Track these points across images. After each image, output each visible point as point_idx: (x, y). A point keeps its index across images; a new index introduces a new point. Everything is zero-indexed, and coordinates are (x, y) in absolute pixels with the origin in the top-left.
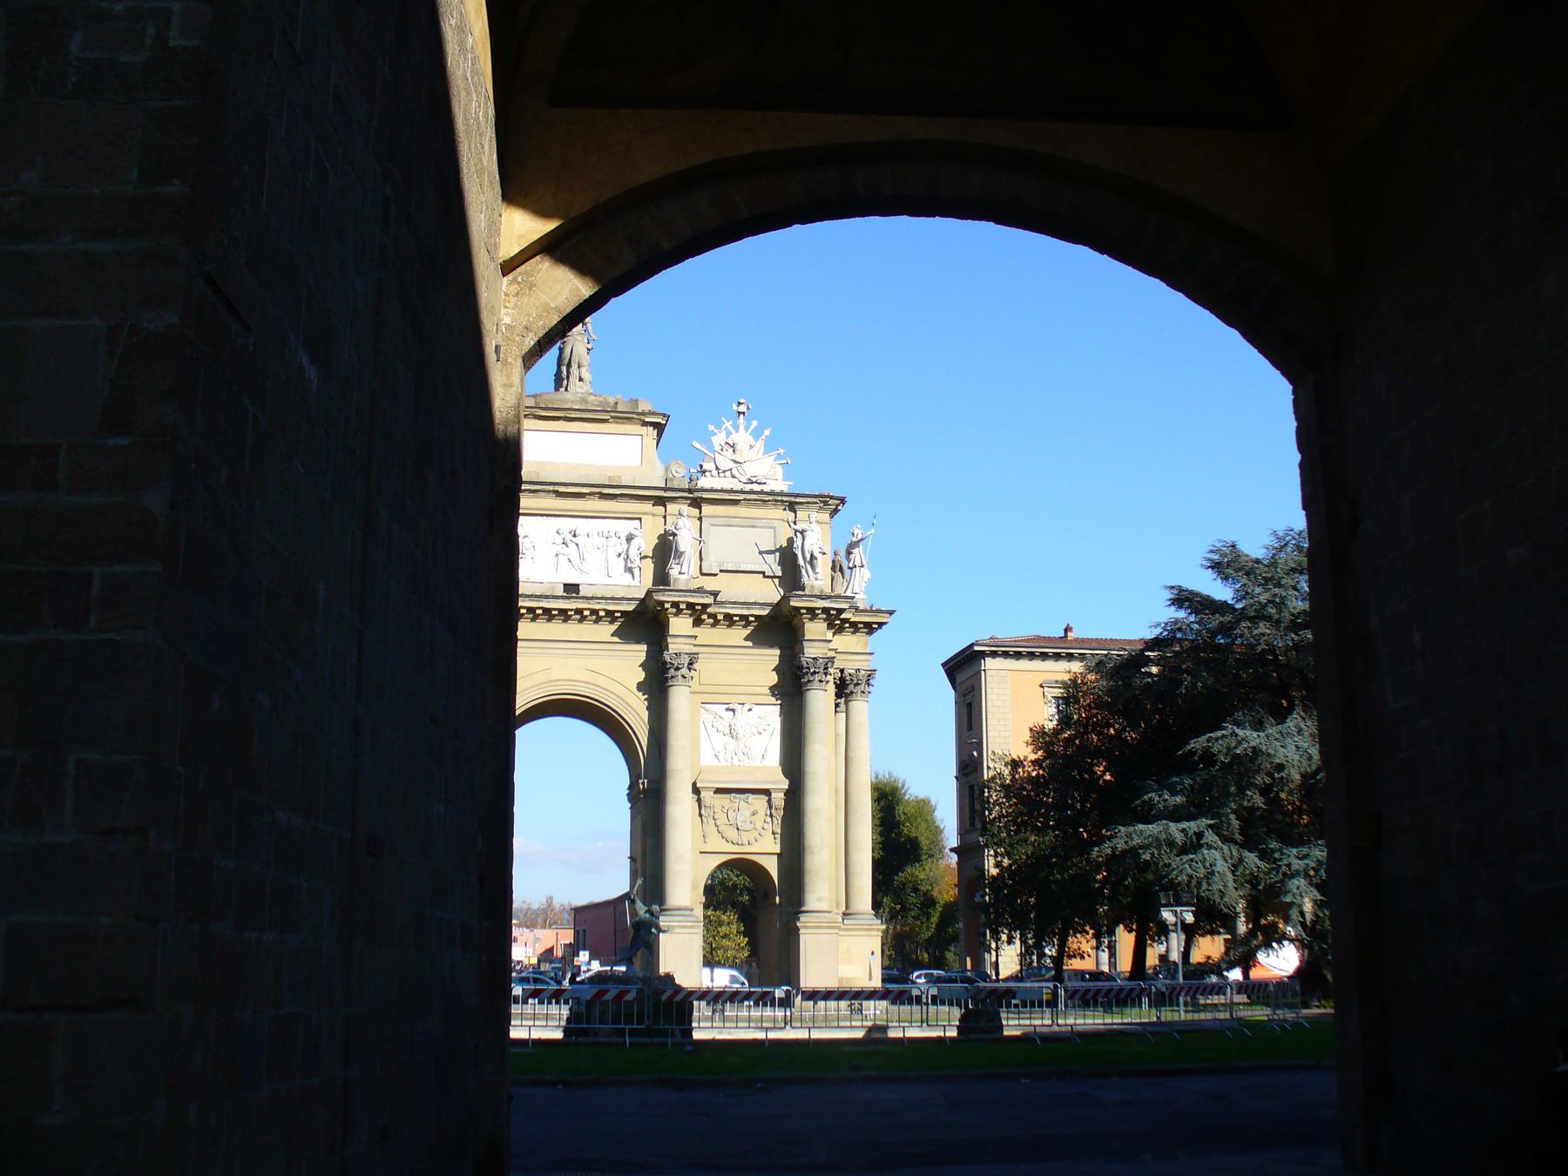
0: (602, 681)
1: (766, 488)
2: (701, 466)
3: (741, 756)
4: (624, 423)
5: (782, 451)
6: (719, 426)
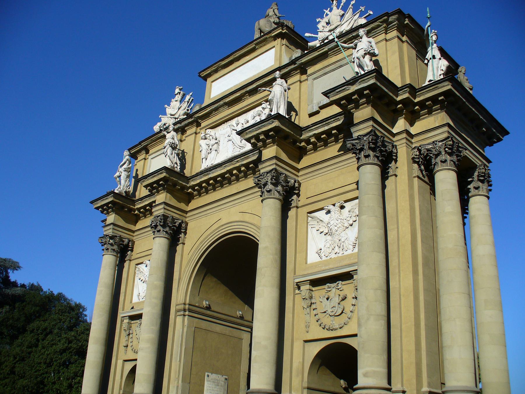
0: (247, 218)
3: (337, 250)
4: (265, 45)
5: (363, 8)
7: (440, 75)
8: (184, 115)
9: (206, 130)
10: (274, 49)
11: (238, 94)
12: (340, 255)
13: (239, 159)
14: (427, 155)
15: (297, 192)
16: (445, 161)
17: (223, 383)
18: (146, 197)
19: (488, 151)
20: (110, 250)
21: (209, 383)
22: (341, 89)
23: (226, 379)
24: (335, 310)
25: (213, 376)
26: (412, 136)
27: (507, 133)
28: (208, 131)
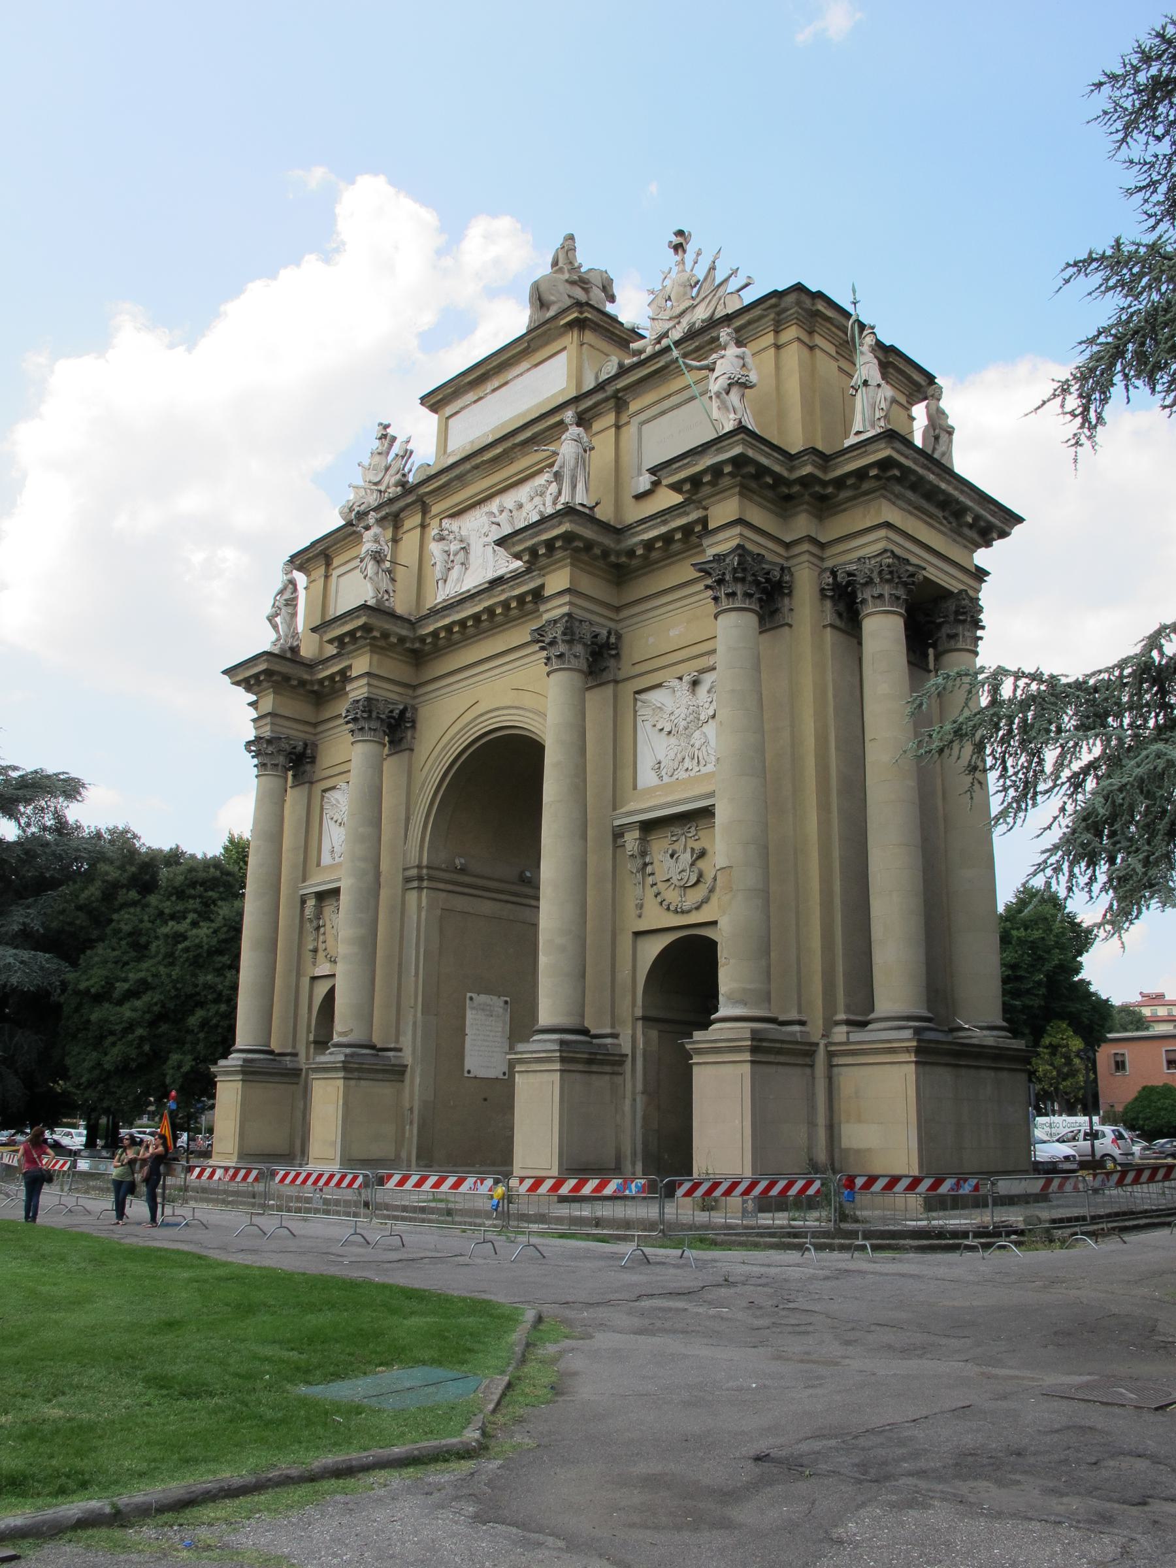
0: (528, 700)
3: (687, 763)
7: (879, 419)
8: (396, 485)
9: (441, 520)
10: (564, 354)
11: (498, 450)
12: (692, 774)
13: (505, 586)
14: (849, 583)
15: (613, 652)
16: (881, 596)
17: (501, 1010)
18: (333, 657)
19: (982, 557)
20: (269, 765)
21: (474, 1012)
22: (680, 464)
23: (506, 1002)
24: (685, 875)
25: (482, 999)
26: (822, 546)
27: (1019, 520)
28: (446, 523)
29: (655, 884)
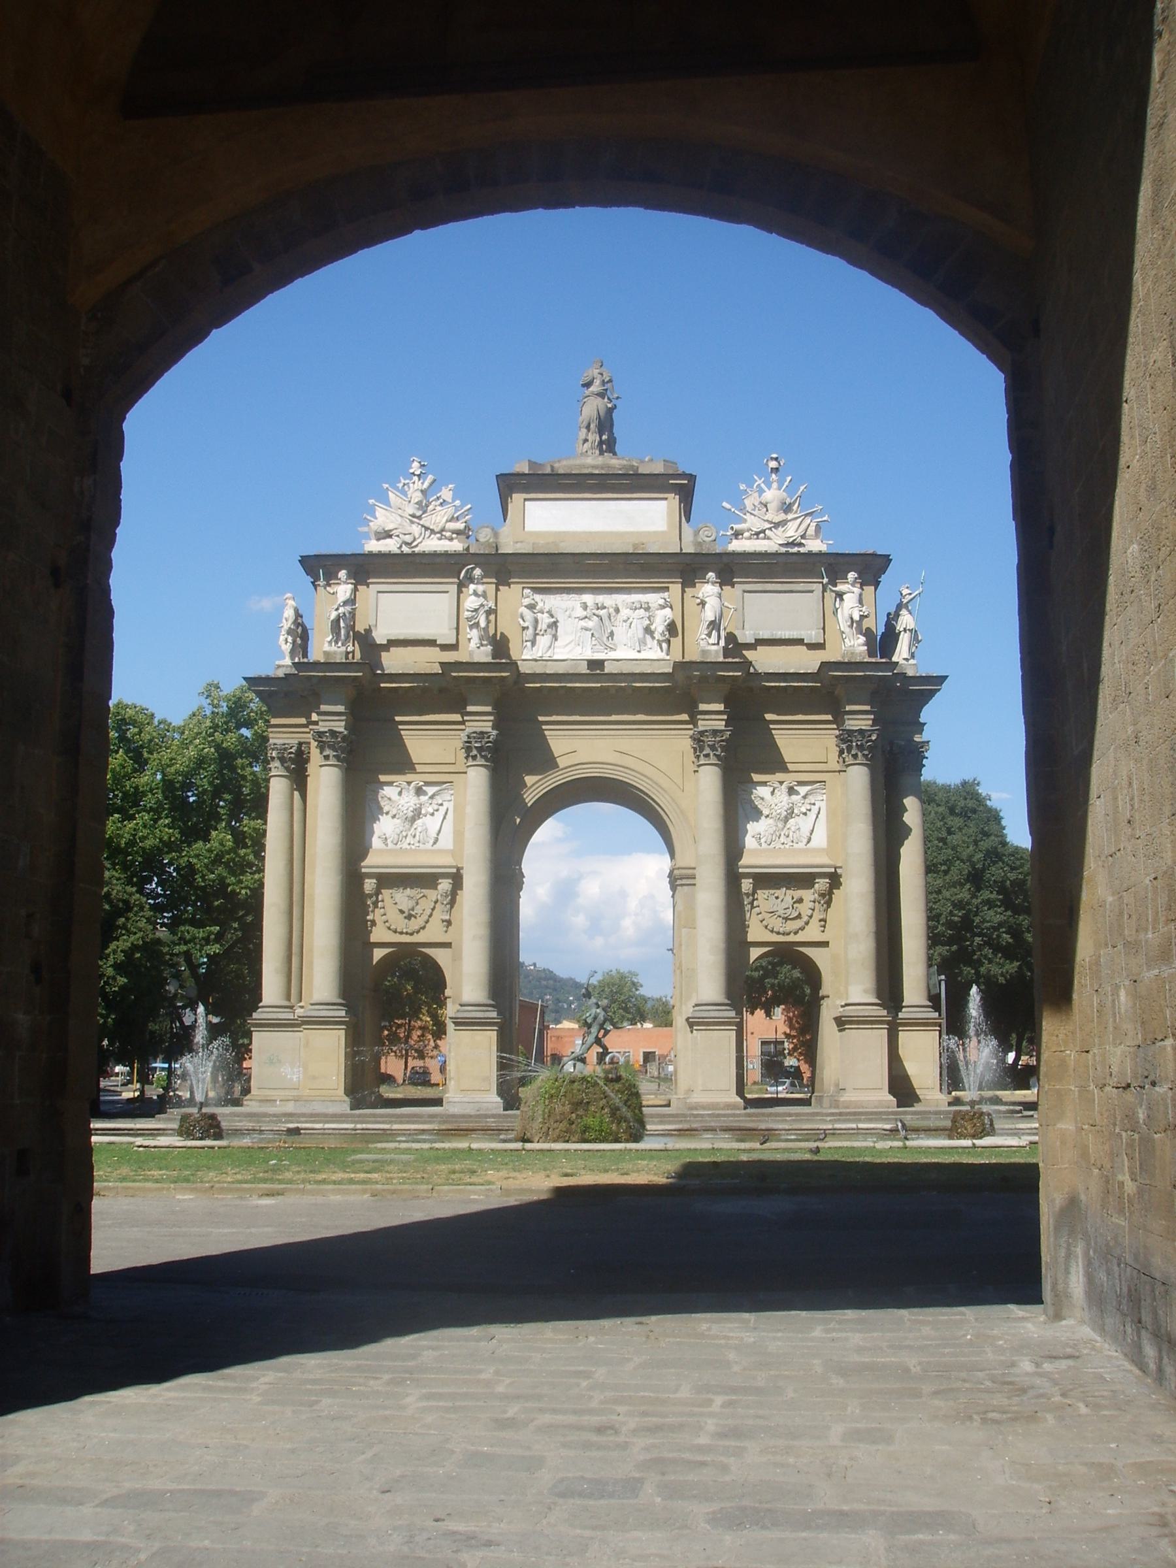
1: (802, 550)
2: (732, 528)
6: (750, 486)
9: (523, 588)
24: (788, 912)
29: (760, 913)
